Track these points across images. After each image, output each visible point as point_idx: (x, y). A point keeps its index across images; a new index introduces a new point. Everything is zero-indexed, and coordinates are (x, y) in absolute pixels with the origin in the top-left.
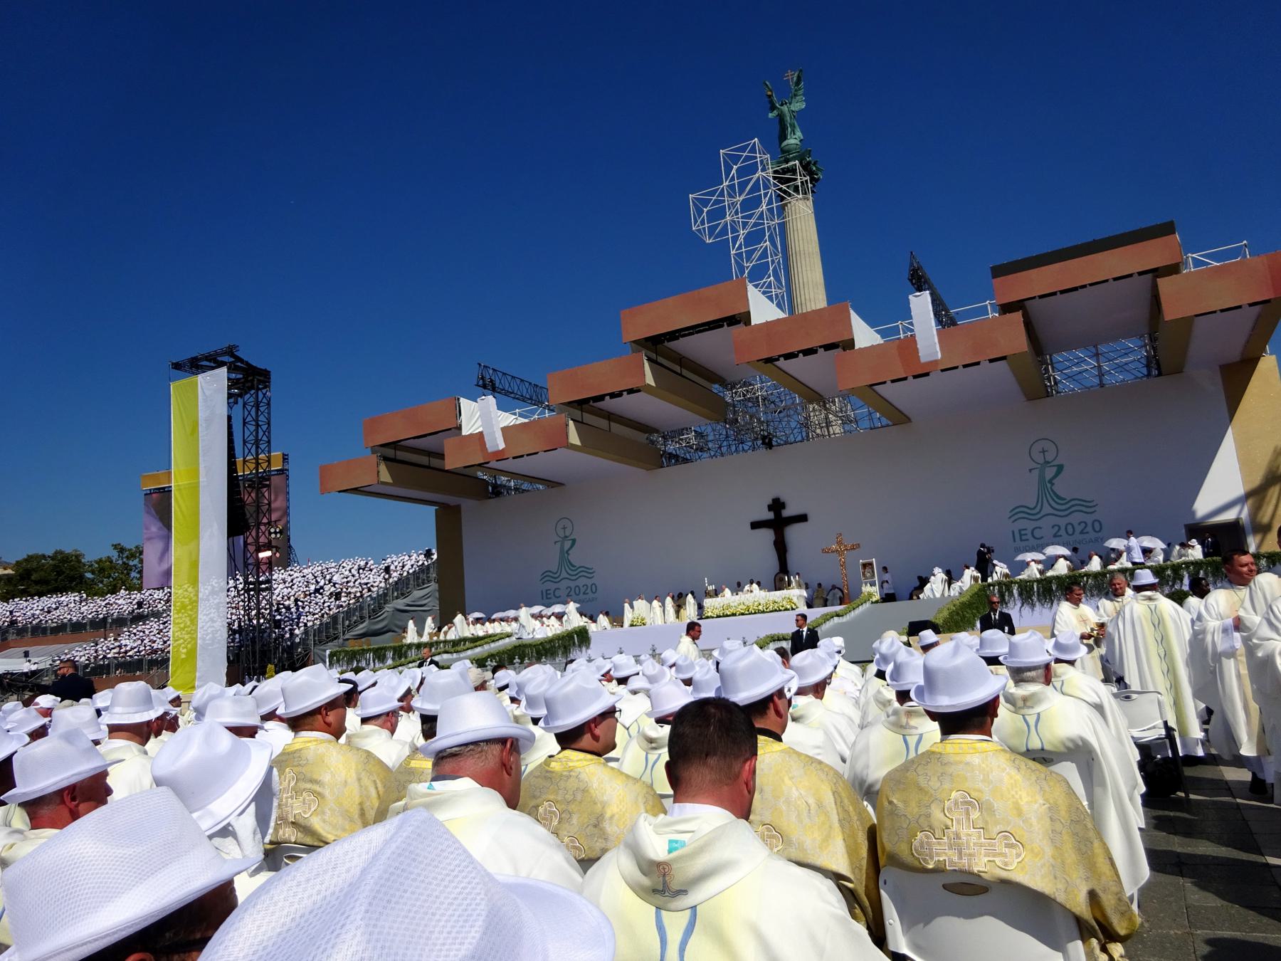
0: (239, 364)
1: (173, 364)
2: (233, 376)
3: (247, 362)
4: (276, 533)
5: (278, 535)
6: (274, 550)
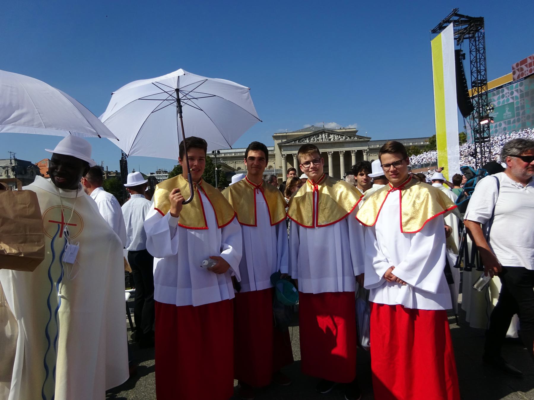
0: (462, 19)
1: (432, 31)
2: (458, 28)
3: (467, 17)
4: (490, 109)
5: (492, 111)
6: (490, 119)
